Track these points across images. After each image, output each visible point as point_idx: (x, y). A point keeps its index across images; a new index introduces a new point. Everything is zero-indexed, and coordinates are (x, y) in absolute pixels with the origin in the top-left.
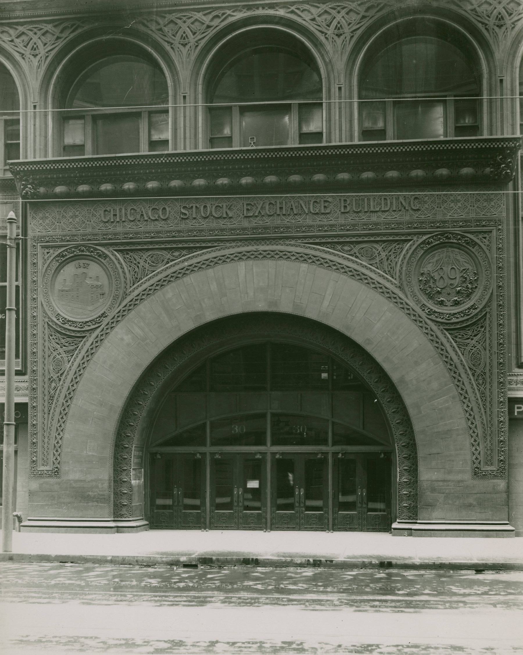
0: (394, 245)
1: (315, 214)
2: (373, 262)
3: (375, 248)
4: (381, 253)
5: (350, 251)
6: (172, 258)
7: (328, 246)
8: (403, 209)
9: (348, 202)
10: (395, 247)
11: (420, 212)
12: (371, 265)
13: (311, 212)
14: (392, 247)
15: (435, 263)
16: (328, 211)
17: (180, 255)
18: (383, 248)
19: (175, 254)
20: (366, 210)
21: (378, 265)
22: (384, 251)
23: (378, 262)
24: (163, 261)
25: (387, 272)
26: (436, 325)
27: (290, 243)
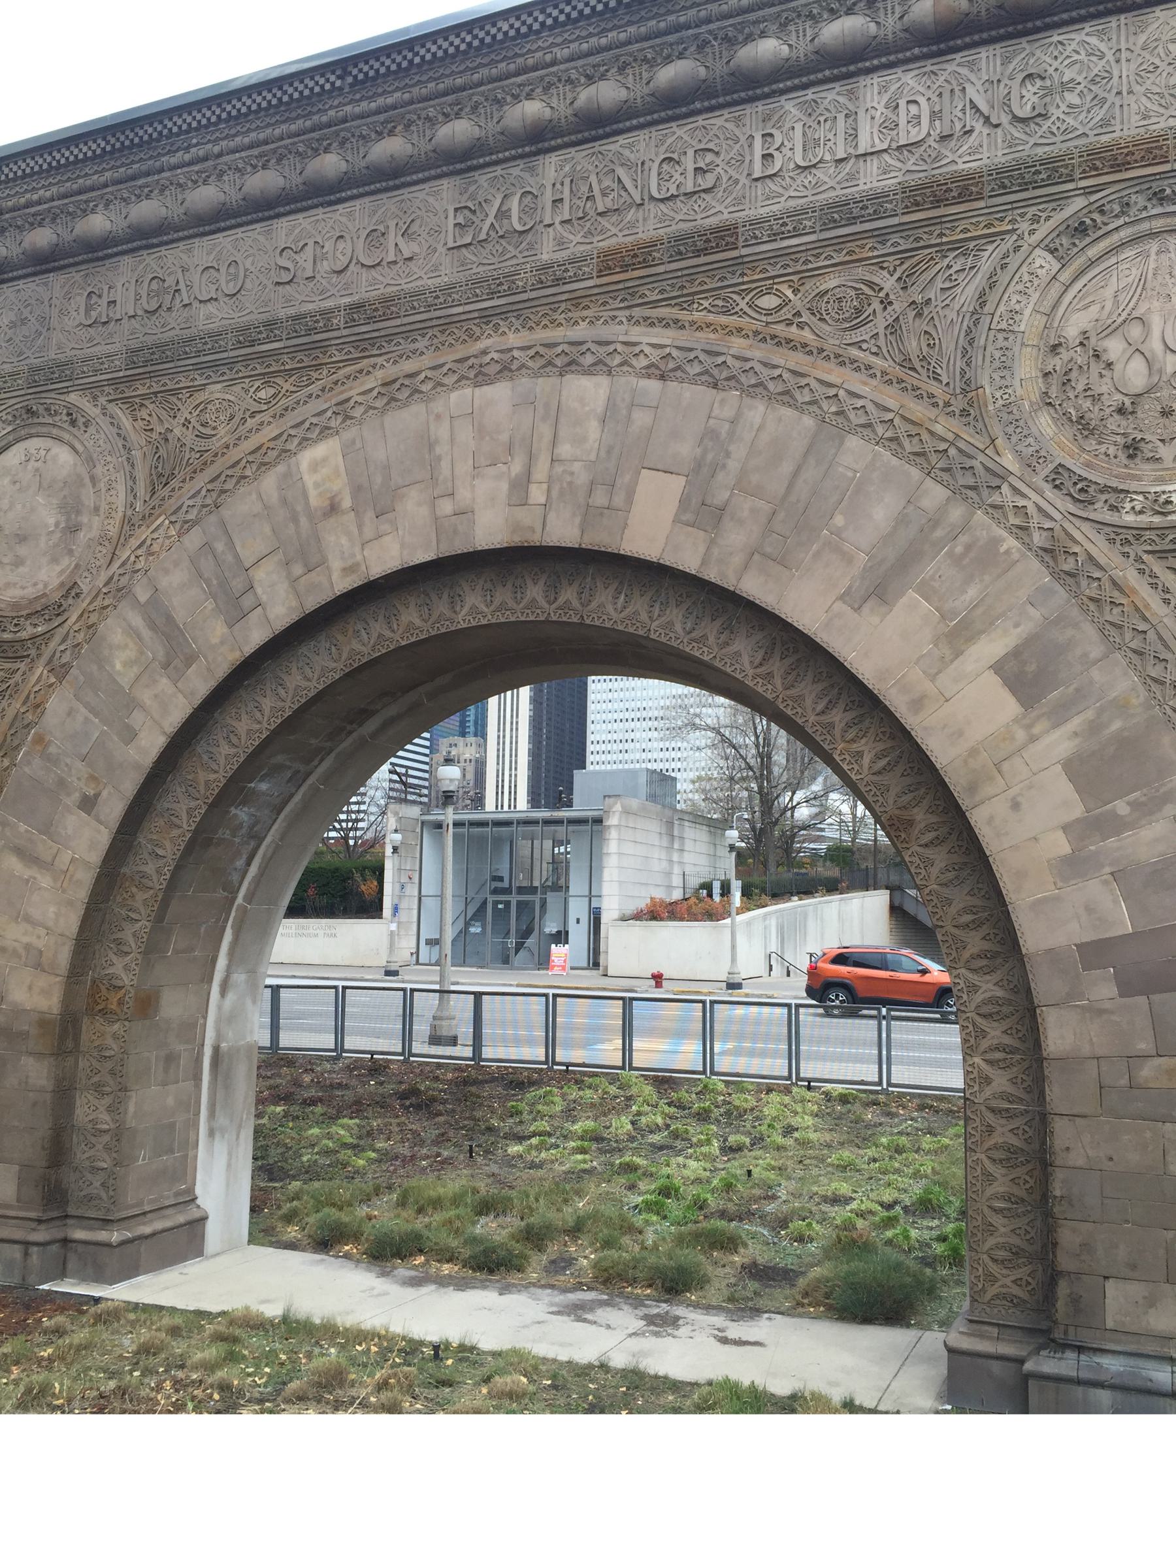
0: (946, 262)
1: (662, 200)
2: (863, 334)
3: (870, 284)
4: (892, 297)
5: (779, 308)
6: (255, 407)
7: (706, 304)
8: (979, 126)
9: (778, 139)
10: (949, 267)
11: (1049, 123)
12: (858, 345)
13: (652, 198)
14: (938, 267)
15: (1109, 305)
16: (708, 181)
17: (274, 396)
18: (900, 279)
19: (262, 394)
20: (841, 154)
21: (882, 341)
22: (904, 288)
23: (881, 331)
24: (232, 418)
25: (917, 365)
26: (1112, 541)
27: (585, 313)
